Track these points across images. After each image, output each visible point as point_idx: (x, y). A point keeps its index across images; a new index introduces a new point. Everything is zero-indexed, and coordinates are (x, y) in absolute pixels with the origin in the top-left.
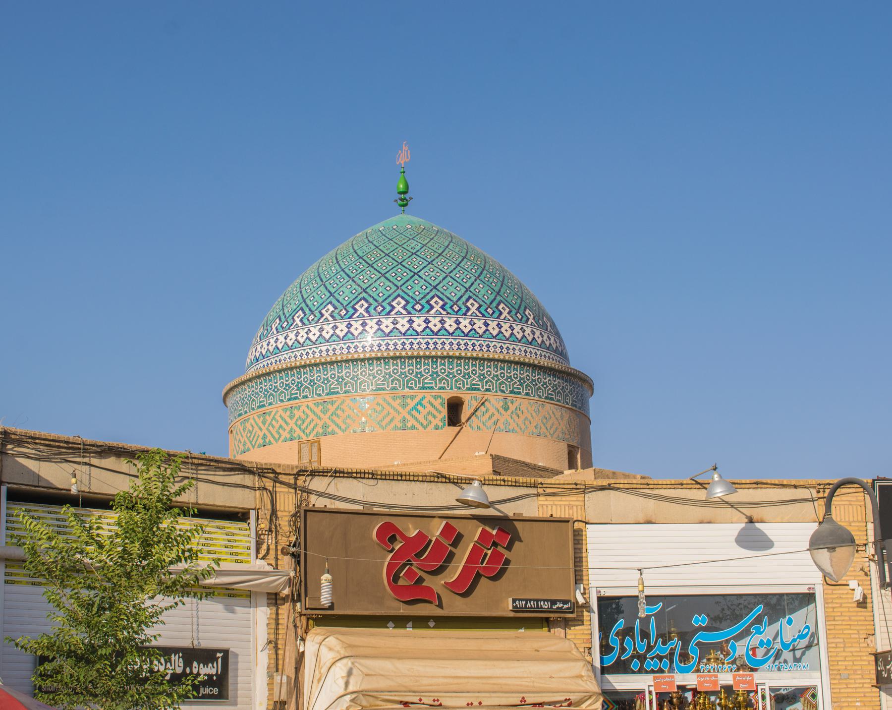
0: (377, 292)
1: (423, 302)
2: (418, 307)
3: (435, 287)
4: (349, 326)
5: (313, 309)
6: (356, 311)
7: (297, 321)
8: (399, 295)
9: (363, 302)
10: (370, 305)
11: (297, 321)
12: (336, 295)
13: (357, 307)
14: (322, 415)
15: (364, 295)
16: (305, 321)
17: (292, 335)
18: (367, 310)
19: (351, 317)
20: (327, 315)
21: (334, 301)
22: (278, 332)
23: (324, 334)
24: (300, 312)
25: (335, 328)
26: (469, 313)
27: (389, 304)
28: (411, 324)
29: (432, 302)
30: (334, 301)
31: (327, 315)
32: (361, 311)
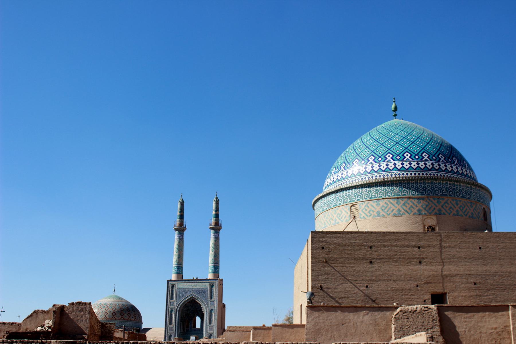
1: (401, 155)
4: (402, 164)
6: (405, 157)
7: (371, 161)
9: (407, 153)
13: (405, 155)
15: (407, 150)
16: (376, 160)
18: (410, 157)
19: (403, 160)
20: (389, 158)
23: (374, 168)
24: (372, 157)
25: (395, 164)
31: (389, 158)
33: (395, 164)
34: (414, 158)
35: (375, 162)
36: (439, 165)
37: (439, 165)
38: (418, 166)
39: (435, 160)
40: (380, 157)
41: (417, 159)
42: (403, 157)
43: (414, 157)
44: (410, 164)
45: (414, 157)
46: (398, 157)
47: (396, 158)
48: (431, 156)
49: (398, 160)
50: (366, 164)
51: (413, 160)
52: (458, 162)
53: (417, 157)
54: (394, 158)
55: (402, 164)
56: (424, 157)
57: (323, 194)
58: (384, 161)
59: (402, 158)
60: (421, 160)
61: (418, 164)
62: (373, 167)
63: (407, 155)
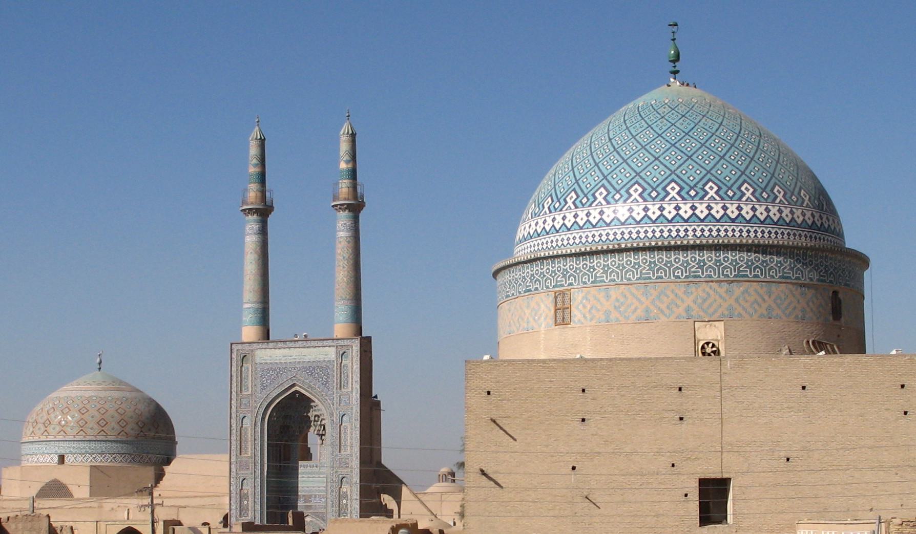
0: (688, 175)
2: (654, 194)
3: (709, 172)
5: (618, 188)
9: (673, 184)
11: (600, 198)
12: (609, 177)
13: (668, 189)
14: (766, 298)
17: (595, 213)
18: (678, 193)
19: (663, 200)
21: (641, 181)
22: (576, 207)
25: (646, 209)
26: (778, 201)
27: (627, 192)
28: (694, 210)
29: (668, 189)
30: (641, 181)
32: (673, 194)
33: (646, 209)
34: (686, 196)
35: (608, 203)
36: (739, 208)
37: (739, 208)
39: (731, 198)
41: (693, 198)
43: (688, 193)
46: (654, 194)
47: (649, 195)
48: (724, 188)
49: (654, 199)
50: (590, 205)
51: (683, 199)
55: (661, 209)
56: (707, 193)
57: (507, 263)
58: (625, 202)
59: (661, 197)
60: (702, 199)
61: (693, 208)
62: (602, 213)
63: (673, 189)
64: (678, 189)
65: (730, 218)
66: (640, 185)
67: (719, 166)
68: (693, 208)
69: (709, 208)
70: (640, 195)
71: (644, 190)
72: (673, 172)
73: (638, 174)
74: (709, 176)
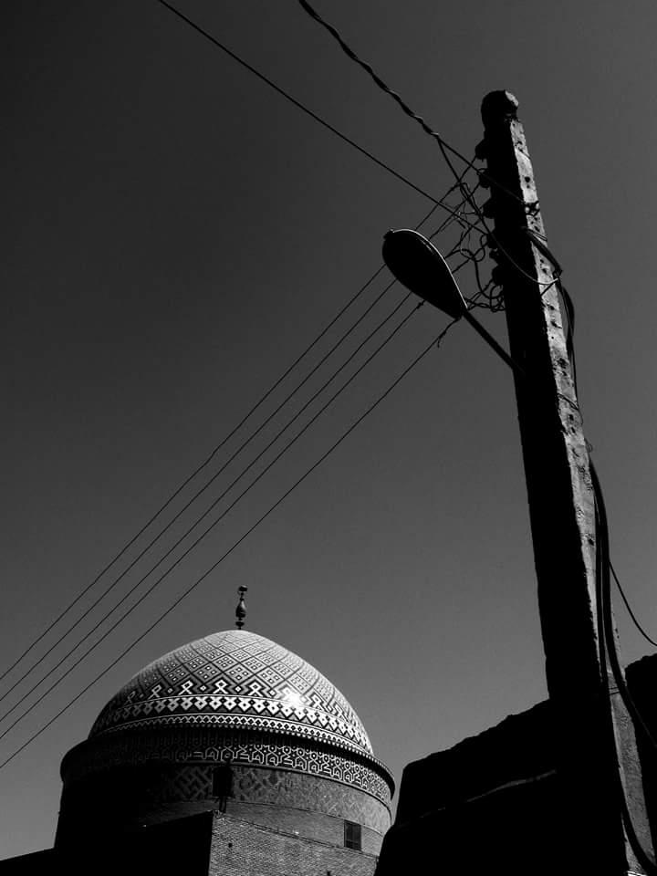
4: (209, 700)
5: (172, 683)
8: (255, 681)
9: (222, 681)
10: (229, 685)
13: (217, 684)
19: (211, 692)
20: (186, 689)
21: (193, 678)
25: (194, 701)
30: (193, 678)
38: (237, 706)
40: (171, 687)
41: (238, 693)
42: (212, 688)
43: (234, 689)
44: (223, 700)
45: (268, 692)
46: (203, 688)
47: (199, 688)
49: (203, 692)
51: (230, 693)
52: (321, 704)
53: (238, 689)
54: (194, 689)
55: (209, 700)
56: (251, 690)
58: (176, 694)
60: (246, 694)
61: (238, 701)
63: (221, 684)
64: (225, 684)
65: (284, 715)
66: (192, 681)
67: (264, 671)
68: (238, 701)
69: (252, 702)
70: (190, 689)
71: (195, 684)
72: (223, 672)
73: (192, 673)
74: (255, 677)
